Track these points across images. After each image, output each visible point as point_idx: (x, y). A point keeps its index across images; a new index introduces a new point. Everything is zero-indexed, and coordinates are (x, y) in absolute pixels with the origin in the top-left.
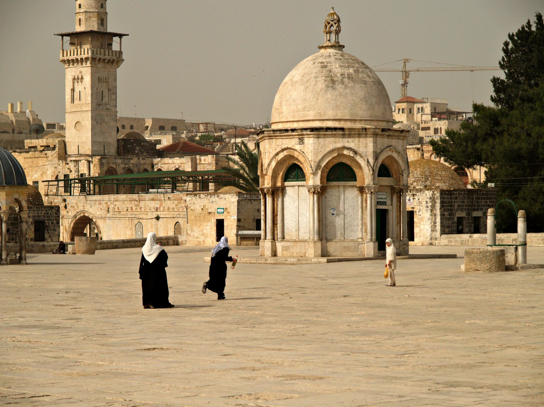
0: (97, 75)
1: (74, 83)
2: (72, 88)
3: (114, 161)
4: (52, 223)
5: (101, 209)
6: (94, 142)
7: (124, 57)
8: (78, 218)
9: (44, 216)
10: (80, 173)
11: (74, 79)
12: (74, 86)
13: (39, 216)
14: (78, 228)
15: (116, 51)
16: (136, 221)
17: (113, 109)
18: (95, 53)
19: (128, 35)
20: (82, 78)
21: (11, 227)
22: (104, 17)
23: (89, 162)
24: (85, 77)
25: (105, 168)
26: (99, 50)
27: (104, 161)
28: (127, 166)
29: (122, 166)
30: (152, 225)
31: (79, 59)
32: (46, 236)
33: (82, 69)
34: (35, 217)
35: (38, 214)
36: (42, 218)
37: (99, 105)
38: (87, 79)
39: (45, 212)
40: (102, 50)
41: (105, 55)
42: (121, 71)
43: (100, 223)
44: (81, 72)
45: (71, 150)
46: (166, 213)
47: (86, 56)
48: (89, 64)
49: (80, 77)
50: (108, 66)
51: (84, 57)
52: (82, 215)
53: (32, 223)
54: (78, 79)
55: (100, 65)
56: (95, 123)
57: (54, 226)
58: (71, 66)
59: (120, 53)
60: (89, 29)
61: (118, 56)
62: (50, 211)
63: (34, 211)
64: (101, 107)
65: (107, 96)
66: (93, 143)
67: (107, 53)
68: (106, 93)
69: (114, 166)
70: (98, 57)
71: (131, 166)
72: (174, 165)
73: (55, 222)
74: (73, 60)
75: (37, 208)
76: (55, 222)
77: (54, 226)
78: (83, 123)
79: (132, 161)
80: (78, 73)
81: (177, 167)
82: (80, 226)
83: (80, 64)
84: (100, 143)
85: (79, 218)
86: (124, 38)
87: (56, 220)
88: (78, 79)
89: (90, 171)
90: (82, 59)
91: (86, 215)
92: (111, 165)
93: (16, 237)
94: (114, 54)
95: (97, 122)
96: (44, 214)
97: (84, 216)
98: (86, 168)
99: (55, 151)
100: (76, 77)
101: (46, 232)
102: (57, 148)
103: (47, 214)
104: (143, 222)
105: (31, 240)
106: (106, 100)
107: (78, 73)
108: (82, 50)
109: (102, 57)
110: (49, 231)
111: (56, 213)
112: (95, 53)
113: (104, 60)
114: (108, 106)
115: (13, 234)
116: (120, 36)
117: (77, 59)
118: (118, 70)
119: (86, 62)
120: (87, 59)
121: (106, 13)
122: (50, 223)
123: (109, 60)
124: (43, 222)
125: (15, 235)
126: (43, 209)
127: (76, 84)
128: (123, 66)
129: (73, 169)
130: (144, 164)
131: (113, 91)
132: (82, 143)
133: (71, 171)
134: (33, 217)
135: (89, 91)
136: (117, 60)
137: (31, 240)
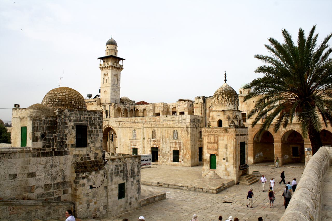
0: (113, 73)
1: (104, 76)
2: (103, 78)
3: (120, 105)
4: (95, 128)
5: (116, 124)
6: (112, 98)
7: (123, 67)
8: (106, 127)
9: (87, 121)
10: (106, 110)
11: (104, 74)
12: (104, 77)
13: (82, 121)
14: (105, 132)
15: (120, 65)
16: (132, 129)
17: (119, 87)
18: (113, 64)
19: (125, 59)
20: (107, 74)
21: (47, 132)
22: (117, 52)
23: (110, 106)
24: (108, 73)
25: (116, 108)
26: (114, 63)
27: (116, 105)
28: (125, 107)
29: (123, 107)
30: (141, 131)
31: (107, 67)
32: (89, 141)
33: (108, 71)
34: (77, 121)
35: (80, 118)
36: (84, 123)
37: (114, 84)
38: (110, 74)
39: (87, 116)
40: (116, 64)
41: (116, 65)
42: (122, 73)
43: (116, 130)
44: (107, 72)
45: (103, 102)
46: (148, 125)
47: (109, 65)
48: (110, 68)
49: (107, 73)
50: (117, 70)
51: (108, 65)
52: (108, 126)
53: (73, 128)
54: (106, 74)
55: (115, 69)
56: (112, 91)
57: (97, 131)
58: (103, 70)
59: (122, 66)
60: (110, 55)
61: (121, 67)
62: (93, 116)
63: (76, 114)
64: (115, 85)
65: (117, 81)
66: (112, 99)
67: (117, 65)
68: (116, 80)
69: (120, 107)
70: (114, 66)
71: (127, 107)
72: (143, 108)
73: (98, 127)
74: (104, 67)
75: (79, 111)
76: (98, 127)
77: (97, 131)
78: (107, 91)
79: (127, 106)
80: (106, 72)
81: (145, 108)
82: (106, 131)
83: (107, 69)
84: (114, 99)
85: (106, 128)
86: (123, 61)
87: (99, 125)
88: (106, 74)
89: (110, 109)
90: (108, 66)
91: (109, 126)
92: (119, 107)
93: (53, 144)
94: (120, 66)
95: (113, 91)
96: (87, 118)
97: (109, 127)
98: (109, 108)
99: (96, 102)
100: (105, 74)
101: (88, 137)
102: (97, 101)
103: (90, 118)
104: (137, 130)
105: (72, 145)
106: (116, 83)
107: (106, 72)
108: (108, 63)
109: (115, 66)
110: (92, 136)
111: (99, 118)
112: (113, 64)
113: (116, 67)
114: (117, 85)
115: (49, 139)
116: (122, 59)
117: (106, 67)
118: (121, 72)
119: (109, 68)
120: (110, 66)
121: (117, 51)
122: (93, 128)
123: (118, 68)
124: (86, 127)
125: (53, 140)
126: (86, 113)
127: (105, 76)
128: (123, 71)
129: (103, 108)
130: (131, 107)
131: (119, 80)
132: (107, 99)
133: (102, 109)
134: (75, 121)
135: (110, 79)
136: (120, 68)
137: (72, 145)
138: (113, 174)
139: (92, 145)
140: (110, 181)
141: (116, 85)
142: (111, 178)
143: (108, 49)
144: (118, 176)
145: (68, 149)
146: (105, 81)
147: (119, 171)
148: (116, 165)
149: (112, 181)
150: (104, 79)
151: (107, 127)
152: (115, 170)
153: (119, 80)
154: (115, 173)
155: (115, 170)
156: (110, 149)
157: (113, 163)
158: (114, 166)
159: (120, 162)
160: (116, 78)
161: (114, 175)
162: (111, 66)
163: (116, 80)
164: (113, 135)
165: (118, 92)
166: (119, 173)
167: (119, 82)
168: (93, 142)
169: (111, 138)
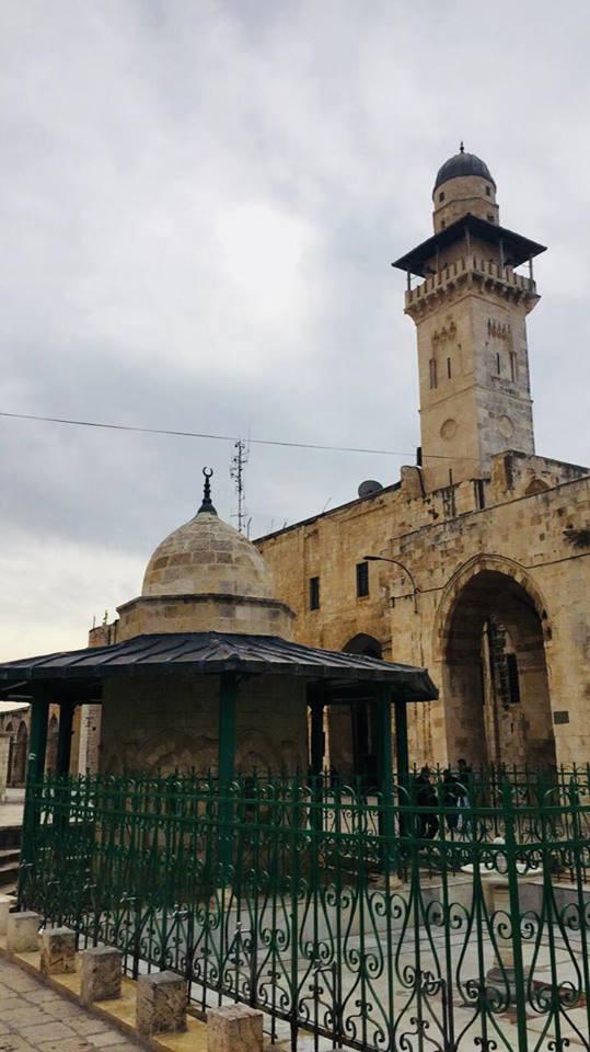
1: (435, 346)
2: (430, 357)
5: (542, 537)
8: (464, 580)
11: (436, 338)
12: (434, 353)
15: (522, 277)
31: (445, 288)
44: (449, 318)
47: (461, 272)
49: (448, 327)
50: (508, 305)
54: (444, 333)
59: (532, 283)
61: (526, 287)
65: (509, 367)
67: (504, 275)
91: (490, 567)
94: (519, 281)
95: (491, 415)
98: (473, 499)
100: (440, 332)
106: (506, 374)
109: (494, 277)
112: (479, 267)
114: (512, 386)
118: (528, 317)
121: (497, 207)
141: (507, 382)
143: (445, 203)
146: (442, 370)
150: (433, 362)
151: (473, 576)
153: (523, 358)
156: (498, 757)
160: (498, 346)
162: (470, 278)
163: (505, 360)
164: (511, 658)
165: (524, 424)
167: (522, 369)
169: (503, 682)
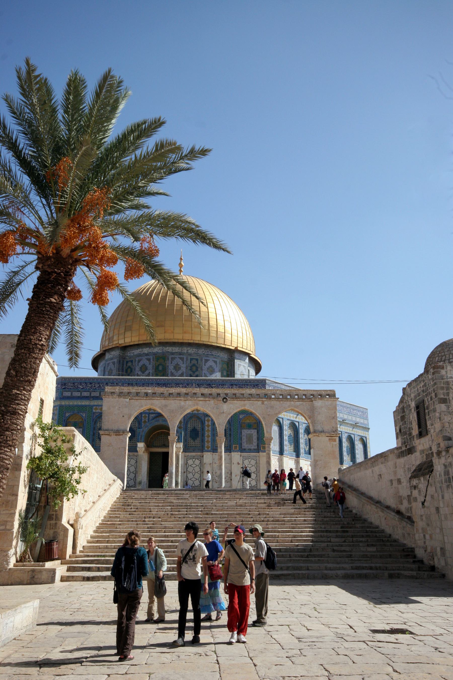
101: (427, 417)
138: (442, 483)
139: (432, 431)
140: (440, 497)
142: (442, 492)
144: (451, 489)
145: (415, 444)
147: (450, 478)
148: (444, 465)
149: (443, 497)
152: (445, 475)
154: (446, 481)
155: (445, 472)
157: (440, 460)
158: (443, 467)
159: (449, 456)
161: (445, 485)
166: (451, 482)
168: (432, 425)
